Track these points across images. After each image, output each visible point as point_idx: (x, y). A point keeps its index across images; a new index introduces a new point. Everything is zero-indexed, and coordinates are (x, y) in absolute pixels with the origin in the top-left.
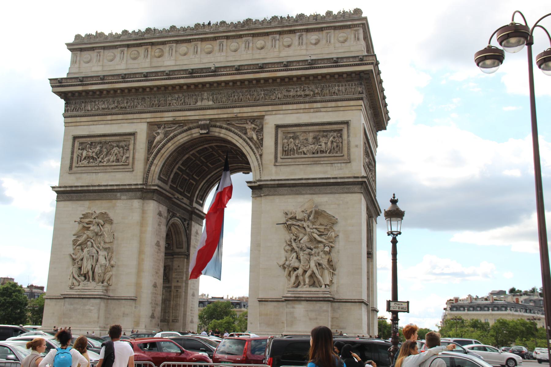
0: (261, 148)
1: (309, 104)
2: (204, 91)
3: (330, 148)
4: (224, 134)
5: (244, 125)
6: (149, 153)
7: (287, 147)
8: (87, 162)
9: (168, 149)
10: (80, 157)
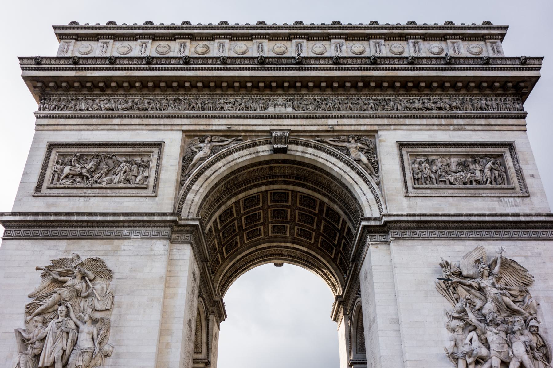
0: (377, 175)
1: (445, 119)
2: (280, 95)
3: (490, 177)
4: (312, 155)
5: (344, 144)
6: (184, 175)
7: (420, 173)
8: (70, 181)
9: (216, 171)
10: (58, 174)
